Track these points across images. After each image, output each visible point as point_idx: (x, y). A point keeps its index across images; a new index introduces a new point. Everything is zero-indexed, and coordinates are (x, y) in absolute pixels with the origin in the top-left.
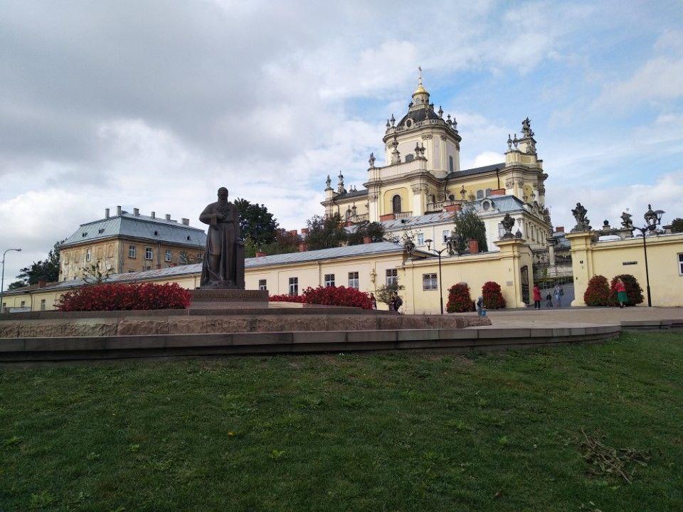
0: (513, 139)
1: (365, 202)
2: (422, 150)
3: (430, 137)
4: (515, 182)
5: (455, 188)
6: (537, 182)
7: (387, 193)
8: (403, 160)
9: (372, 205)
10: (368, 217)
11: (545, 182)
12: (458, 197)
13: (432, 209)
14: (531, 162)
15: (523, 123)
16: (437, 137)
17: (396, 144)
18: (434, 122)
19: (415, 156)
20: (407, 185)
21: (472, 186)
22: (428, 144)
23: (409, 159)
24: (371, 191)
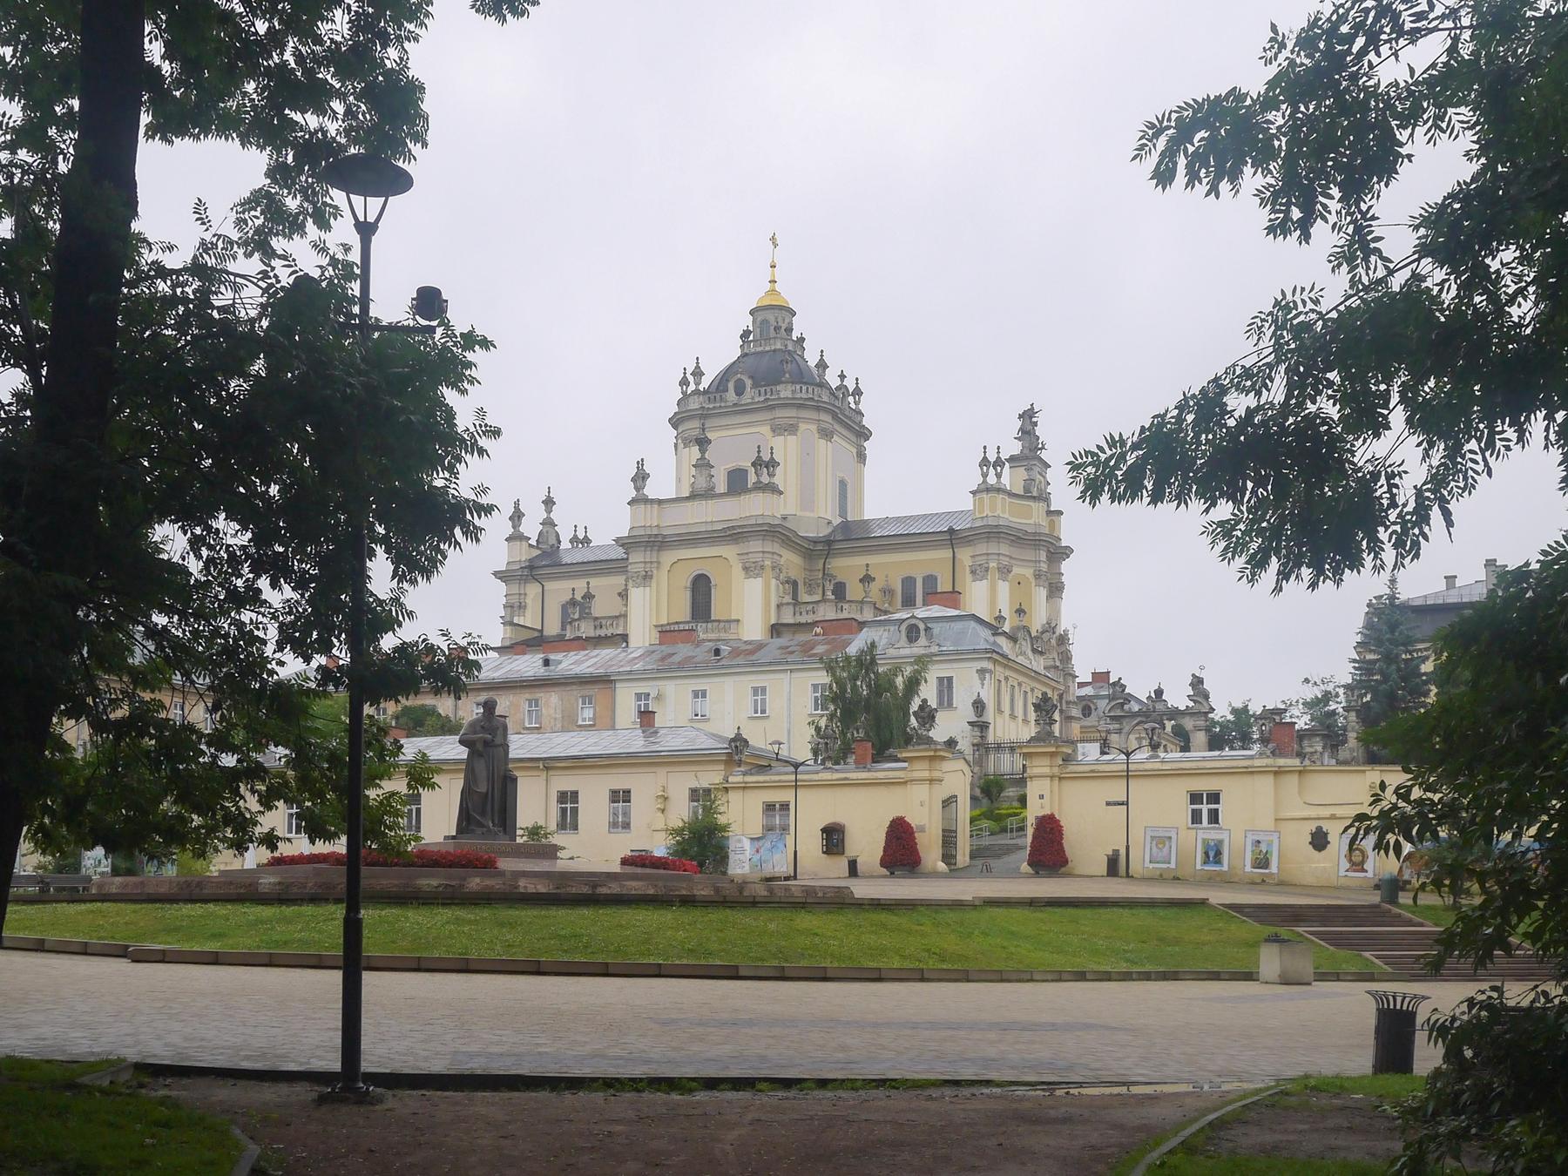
0: (992, 458)
1: (618, 581)
2: (772, 464)
3: (791, 429)
4: (993, 565)
5: (847, 567)
6: (1044, 567)
7: (674, 572)
8: (721, 488)
9: (637, 595)
10: (625, 626)
11: (1065, 566)
12: (854, 591)
13: (788, 618)
14: (1034, 518)
15: (1020, 416)
16: (808, 429)
17: (703, 443)
18: (804, 393)
19: (752, 478)
20: (729, 551)
21: (891, 568)
22: (785, 449)
23: (737, 483)
24: (636, 557)
